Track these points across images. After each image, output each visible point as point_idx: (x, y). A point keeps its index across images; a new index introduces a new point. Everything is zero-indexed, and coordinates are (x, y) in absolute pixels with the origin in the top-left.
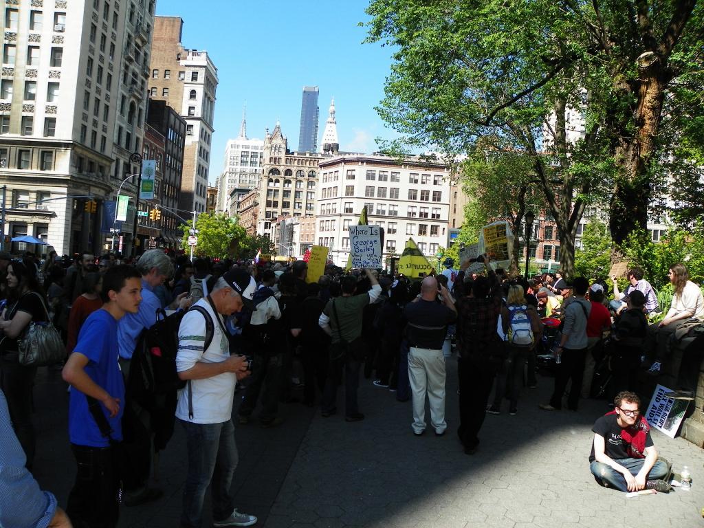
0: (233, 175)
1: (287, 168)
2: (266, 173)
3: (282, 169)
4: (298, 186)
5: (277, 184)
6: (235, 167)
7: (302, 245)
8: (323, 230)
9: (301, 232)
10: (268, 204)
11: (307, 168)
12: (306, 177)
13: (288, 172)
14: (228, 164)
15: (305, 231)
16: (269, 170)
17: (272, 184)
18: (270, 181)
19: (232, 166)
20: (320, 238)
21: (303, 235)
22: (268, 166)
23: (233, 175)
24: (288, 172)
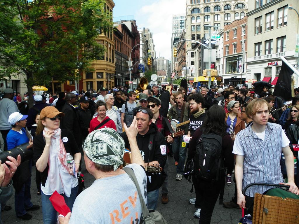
0: (176, 35)
1: (205, 6)
2: (189, 13)
3: (201, 7)
4: (216, 20)
5: (199, 21)
6: (177, 30)
7: (228, 59)
8: (261, 31)
9: (225, 42)
10: (193, 37)
11: (222, 3)
12: (222, 10)
13: (207, 8)
14: (173, 29)
15: (232, 40)
16: (191, 10)
17: (194, 21)
18: (192, 18)
19: (175, 30)
20: (256, 44)
21: (228, 47)
22: (190, 7)
23: (176, 35)
24: (207, 8)
